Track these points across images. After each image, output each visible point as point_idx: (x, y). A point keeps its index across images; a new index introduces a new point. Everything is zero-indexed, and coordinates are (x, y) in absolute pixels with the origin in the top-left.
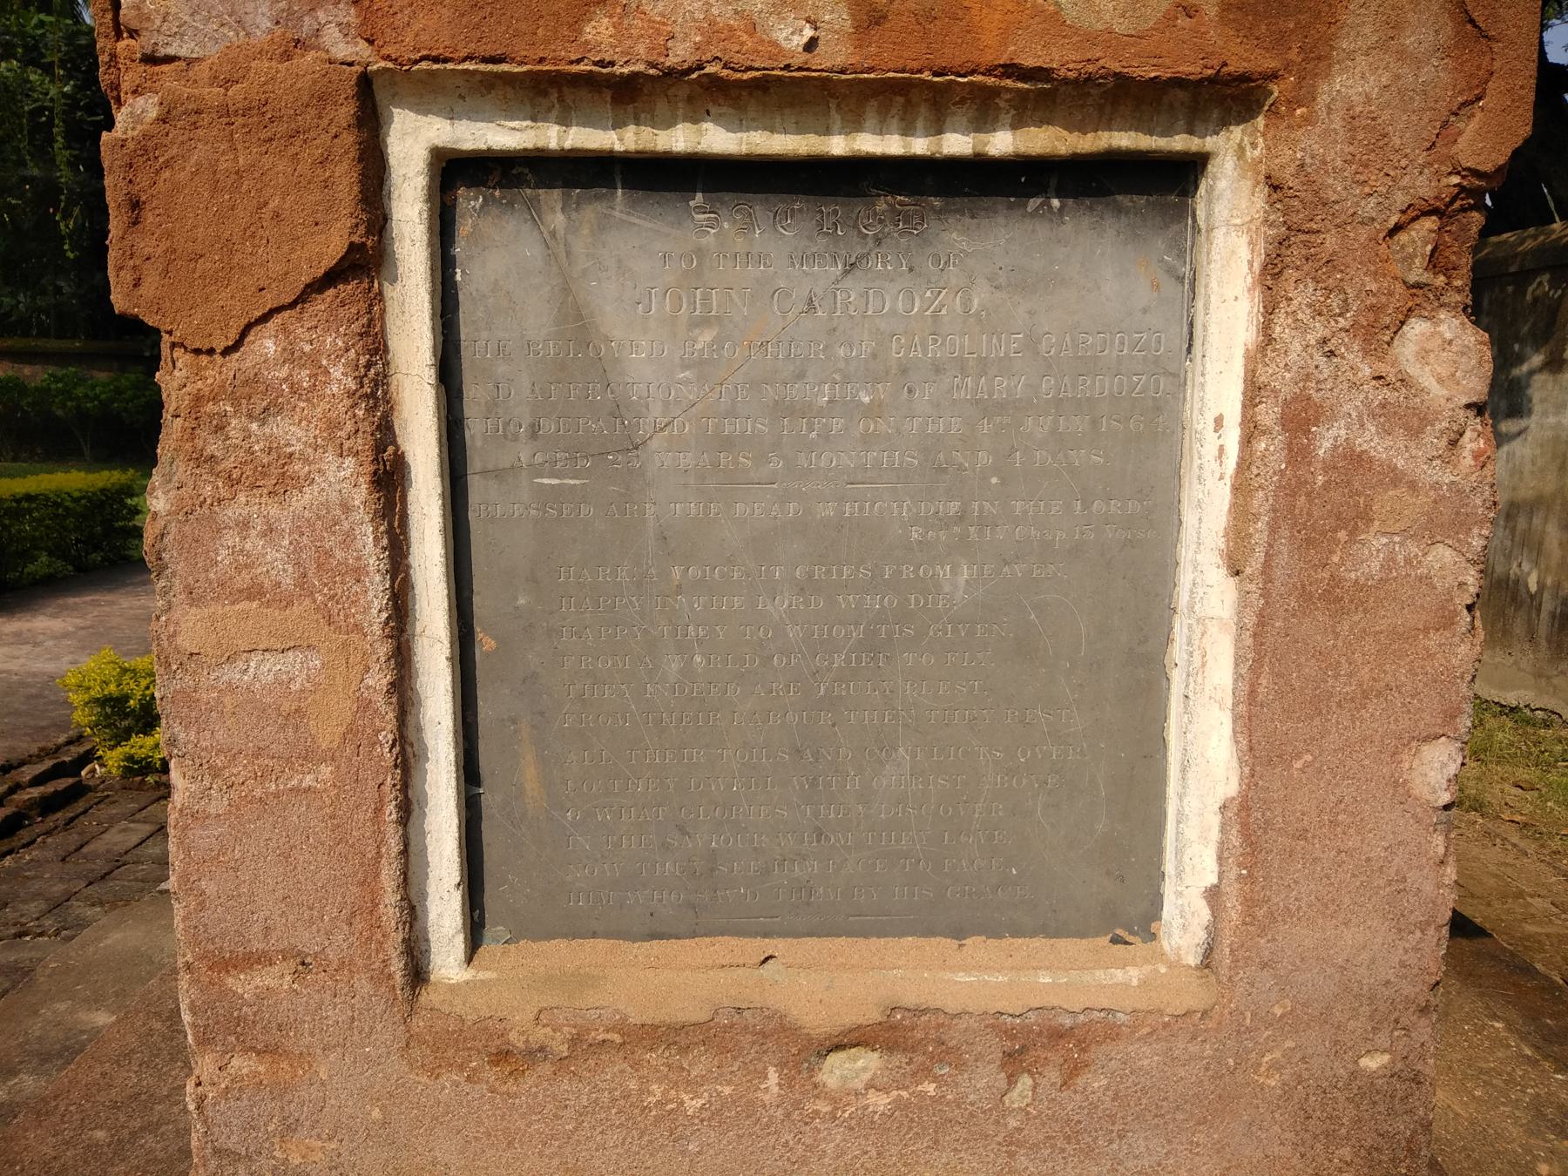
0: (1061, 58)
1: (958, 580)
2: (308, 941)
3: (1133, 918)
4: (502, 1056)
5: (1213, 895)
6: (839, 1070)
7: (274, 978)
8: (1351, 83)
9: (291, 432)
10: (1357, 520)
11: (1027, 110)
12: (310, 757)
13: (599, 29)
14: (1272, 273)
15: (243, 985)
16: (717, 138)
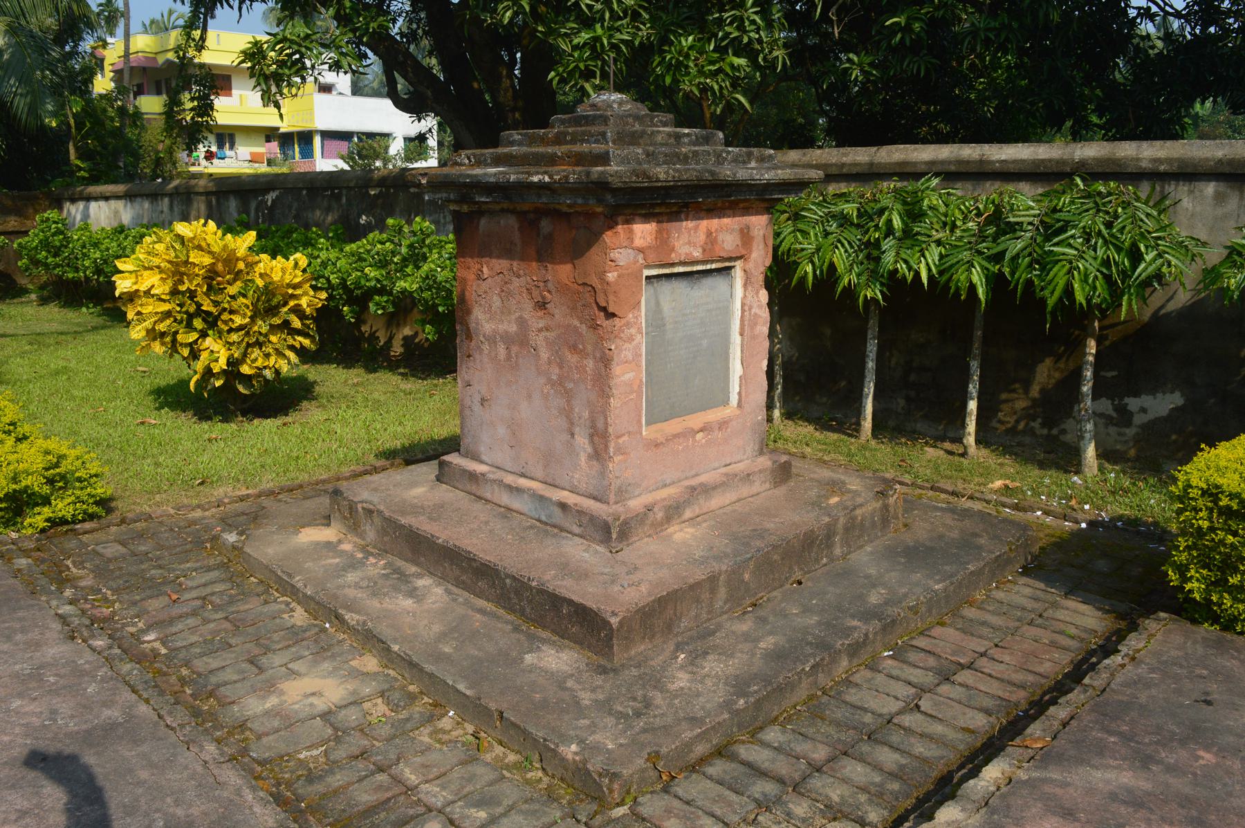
0: (725, 255)
1: (705, 342)
2: (631, 429)
3: (726, 402)
4: (657, 445)
5: (740, 394)
6: (699, 436)
7: (625, 438)
8: (754, 255)
9: (633, 331)
10: (756, 324)
11: (718, 261)
12: (632, 392)
13: (673, 255)
14: (745, 286)
15: (620, 441)
16: (681, 269)
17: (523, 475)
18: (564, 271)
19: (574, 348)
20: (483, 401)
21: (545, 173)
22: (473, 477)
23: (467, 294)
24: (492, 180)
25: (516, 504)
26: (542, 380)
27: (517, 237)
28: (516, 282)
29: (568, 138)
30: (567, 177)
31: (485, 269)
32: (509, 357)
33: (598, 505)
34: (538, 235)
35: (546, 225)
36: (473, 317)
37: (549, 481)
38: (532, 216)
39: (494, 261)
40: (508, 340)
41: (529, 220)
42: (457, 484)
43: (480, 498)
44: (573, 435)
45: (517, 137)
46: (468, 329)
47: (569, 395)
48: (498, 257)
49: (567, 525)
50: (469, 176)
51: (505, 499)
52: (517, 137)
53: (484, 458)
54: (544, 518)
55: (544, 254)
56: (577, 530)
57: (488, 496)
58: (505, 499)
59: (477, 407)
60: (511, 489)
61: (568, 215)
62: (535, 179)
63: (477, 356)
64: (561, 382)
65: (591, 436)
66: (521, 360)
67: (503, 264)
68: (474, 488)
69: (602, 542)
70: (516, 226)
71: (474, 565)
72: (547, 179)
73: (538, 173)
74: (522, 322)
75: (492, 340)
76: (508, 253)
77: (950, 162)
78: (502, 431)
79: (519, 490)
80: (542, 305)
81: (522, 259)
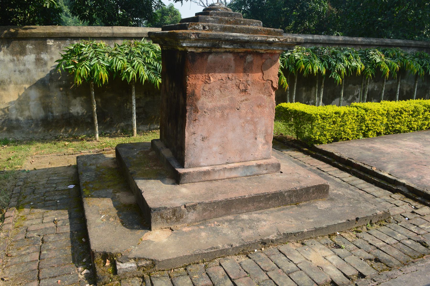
17: (227, 163)
18: (257, 76)
19: (259, 106)
20: (203, 139)
21: (276, 38)
22: (206, 173)
23: (196, 91)
24: (247, 39)
25: (234, 174)
26: (242, 121)
27: (232, 63)
28: (230, 83)
29: (242, 22)
30: (286, 40)
31: (211, 78)
32: (223, 116)
33: (268, 160)
34: (245, 62)
35: (249, 58)
36: (200, 102)
37: (242, 160)
38: (242, 54)
39: (216, 74)
40: (222, 108)
41: (240, 57)
42: (194, 180)
43: (211, 180)
44: (256, 139)
45: (211, 19)
46: (196, 108)
47: (255, 124)
48: (220, 72)
49: (261, 172)
50: (231, 36)
51: (227, 175)
52: (211, 19)
53: (202, 164)
54: (248, 174)
55: (247, 70)
56: (265, 172)
57: (217, 177)
58: (227, 175)
59: (199, 143)
60: (231, 169)
61: (262, 54)
62: (271, 40)
63: (201, 119)
64: (252, 120)
65: (265, 136)
66: (230, 115)
67: (223, 75)
68: (207, 178)
69: (276, 171)
70: (233, 58)
71: (268, 196)
72: (277, 40)
73: (272, 37)
74: (232, 100)
75: (213, 110)
76: (227, 70)
77: (144, 34)
78: (215, 149)
79: (235, 168)
80: (245, 91)
81: (235, 72)
